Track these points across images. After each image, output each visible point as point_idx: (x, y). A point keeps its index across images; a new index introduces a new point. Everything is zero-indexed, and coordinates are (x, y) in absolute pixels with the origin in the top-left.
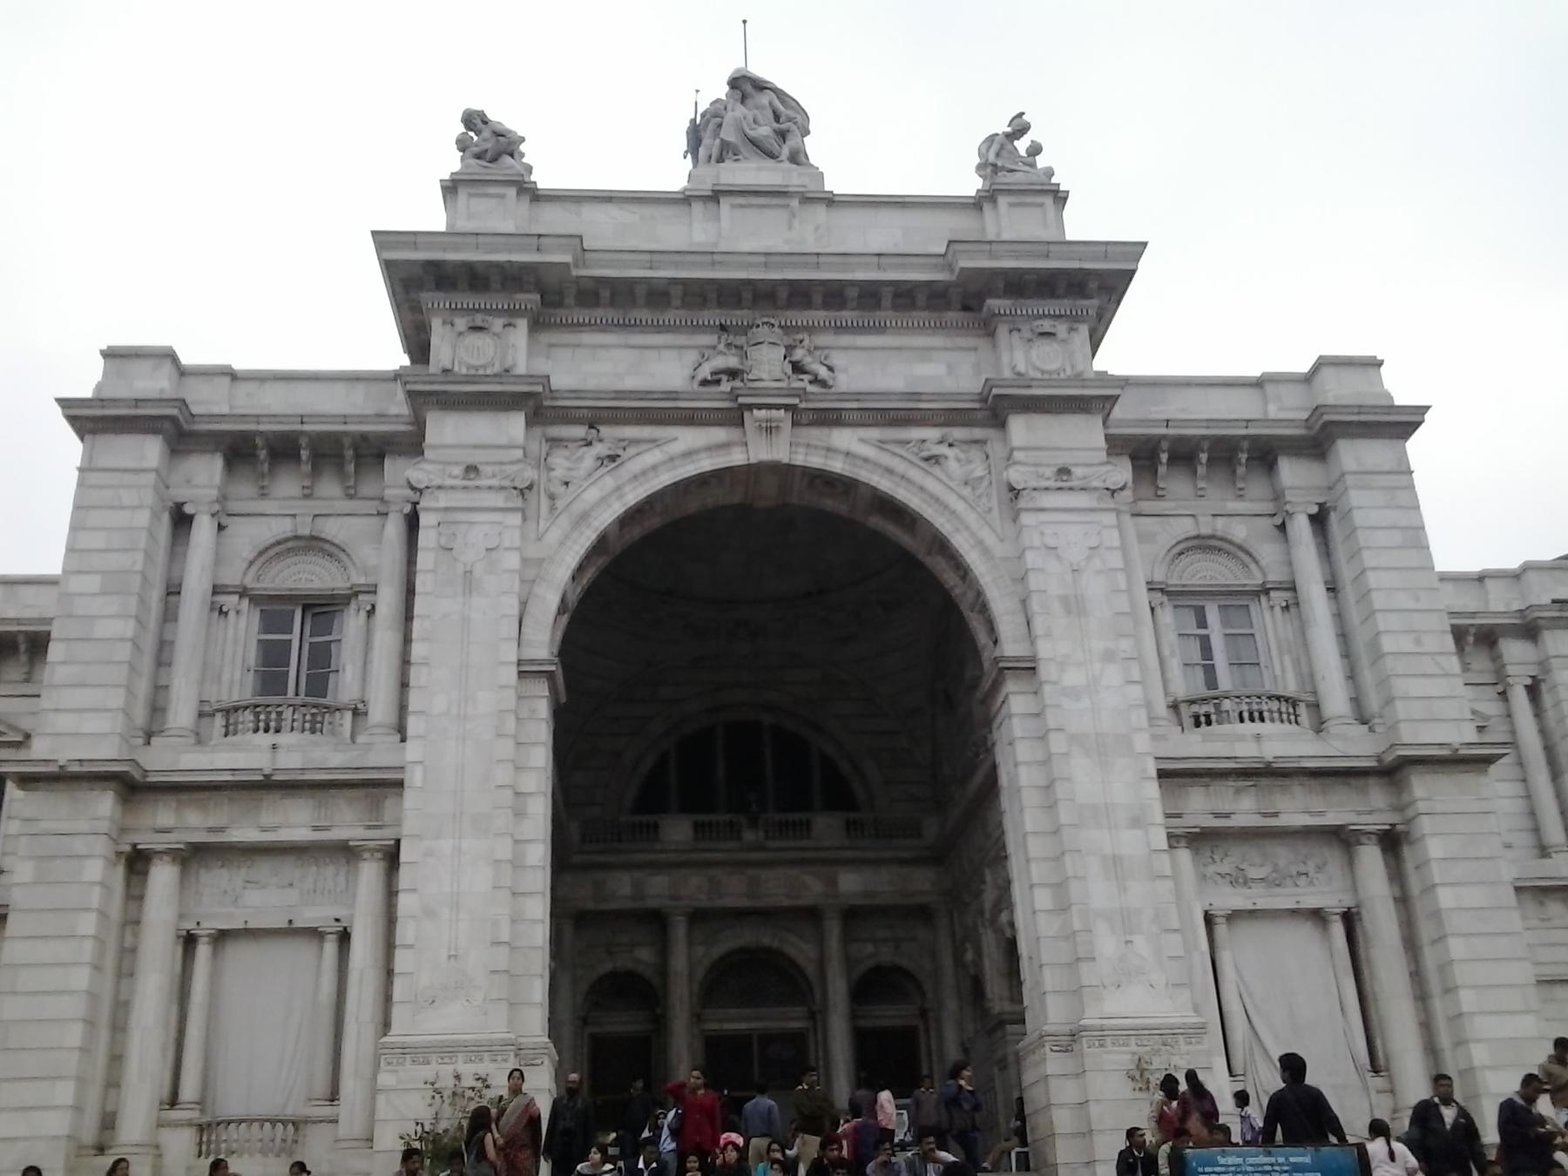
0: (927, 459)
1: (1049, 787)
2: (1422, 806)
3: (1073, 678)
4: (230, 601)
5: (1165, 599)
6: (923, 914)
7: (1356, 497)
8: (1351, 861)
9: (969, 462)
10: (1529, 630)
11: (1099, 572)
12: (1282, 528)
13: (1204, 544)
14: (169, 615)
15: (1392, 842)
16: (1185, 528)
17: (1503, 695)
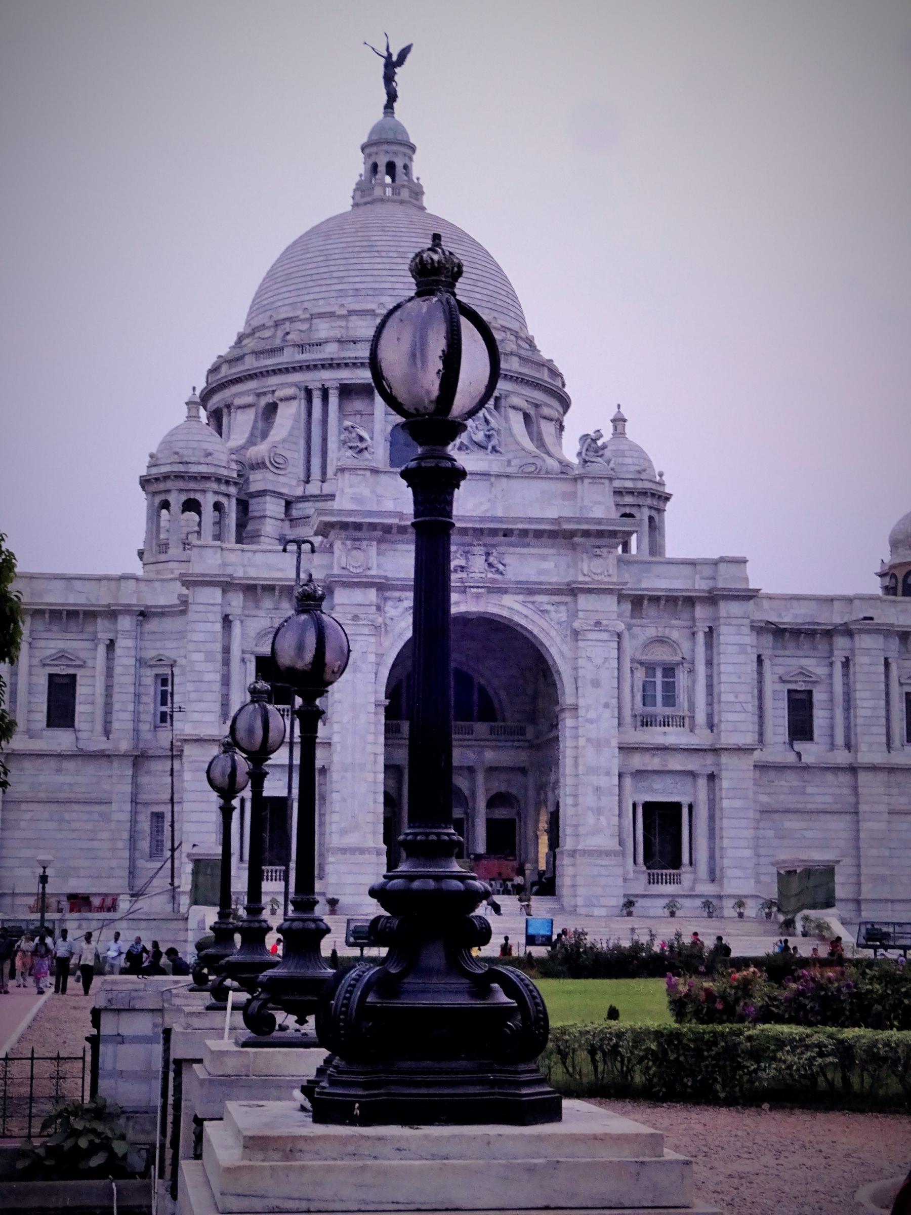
0: (542, 611)
1: (576, 758)
2: (723, 767)
3: (592, 715)
4: (247, 656)
5: (638, 666)
6: (523, 771)
7: (723, 629)
8: (695, 785)
9: (560, 612)
10: (848, 632)
11: (607, 668)
12: (694, 634)
13: (661, 640)
14: (226, 662)
15: (712, 777)
16: (651, 632)
17: (831, 664)
